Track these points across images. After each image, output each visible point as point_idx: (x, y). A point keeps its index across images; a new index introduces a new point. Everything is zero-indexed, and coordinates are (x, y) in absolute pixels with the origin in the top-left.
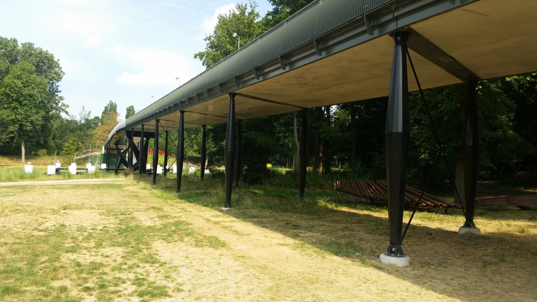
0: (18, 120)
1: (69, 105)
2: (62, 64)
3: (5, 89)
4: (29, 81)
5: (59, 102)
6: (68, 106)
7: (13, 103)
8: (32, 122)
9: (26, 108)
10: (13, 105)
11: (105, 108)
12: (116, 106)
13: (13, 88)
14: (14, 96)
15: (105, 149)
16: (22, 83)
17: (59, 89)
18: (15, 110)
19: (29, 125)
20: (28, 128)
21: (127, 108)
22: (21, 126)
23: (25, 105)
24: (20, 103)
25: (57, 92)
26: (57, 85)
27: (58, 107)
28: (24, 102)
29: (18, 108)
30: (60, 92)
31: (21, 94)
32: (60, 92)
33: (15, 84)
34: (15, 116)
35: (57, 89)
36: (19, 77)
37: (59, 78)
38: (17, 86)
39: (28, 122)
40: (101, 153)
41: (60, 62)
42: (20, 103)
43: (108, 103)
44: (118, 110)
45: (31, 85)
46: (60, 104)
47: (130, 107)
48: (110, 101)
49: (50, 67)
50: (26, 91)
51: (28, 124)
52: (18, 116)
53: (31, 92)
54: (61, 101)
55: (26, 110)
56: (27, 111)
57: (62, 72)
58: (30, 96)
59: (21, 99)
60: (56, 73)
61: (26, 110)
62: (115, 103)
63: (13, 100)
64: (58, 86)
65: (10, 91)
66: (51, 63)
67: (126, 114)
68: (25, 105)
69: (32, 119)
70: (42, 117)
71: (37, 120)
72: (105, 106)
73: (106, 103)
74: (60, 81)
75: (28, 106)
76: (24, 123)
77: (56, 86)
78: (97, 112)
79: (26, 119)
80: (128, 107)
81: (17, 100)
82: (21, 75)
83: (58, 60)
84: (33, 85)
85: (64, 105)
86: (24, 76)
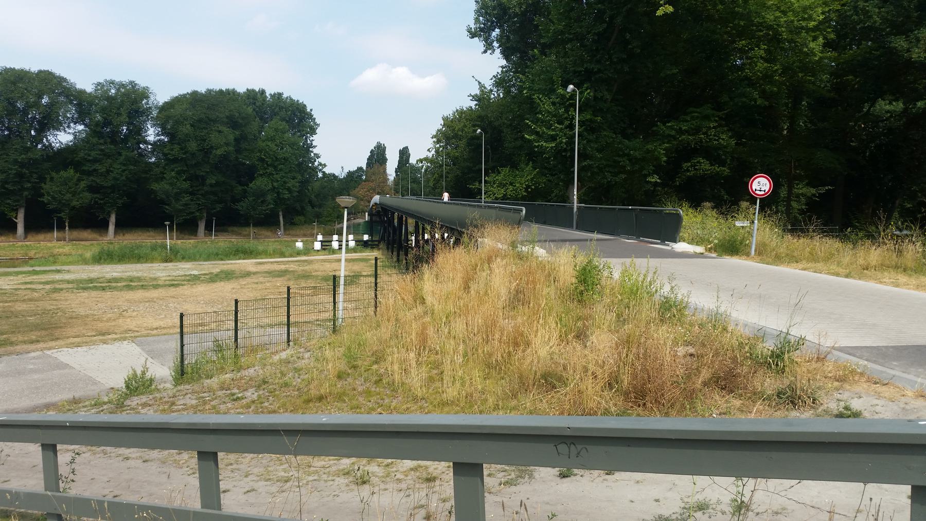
2: (315, 114)
4: (283, 143)
5: (315, 161)
6: (325, 165)
8: (289, 190)
9: (282, 174)
10: (268, 171)
13: (267, 152)
14: (270, 161)
15: (368, 215)
17: (314, 143)
20: (286, 196)
22: (278, 193)
23: (281, 170)
25: (312, 147)
26: (311, 138)
29: (273, 175)
30: (315, 147)
31: (276, 158)
32: (315, 147)
35: (312, 144)
36: (272, 139)
38: (271, 150)
40: (364, 220)
41: (313, 113)
42: (275, 167)
46: (316, 164)
49: (302, 119)
52: (275, 184)
54: (317, 160)
56: (284, 177)
61: (282, 176)
65: (265, 156)
68: (281, 170)
71: (293, 186)
79: (282, 186)
81: (272, 165)
83: (311, 110)
85: (320, 164)
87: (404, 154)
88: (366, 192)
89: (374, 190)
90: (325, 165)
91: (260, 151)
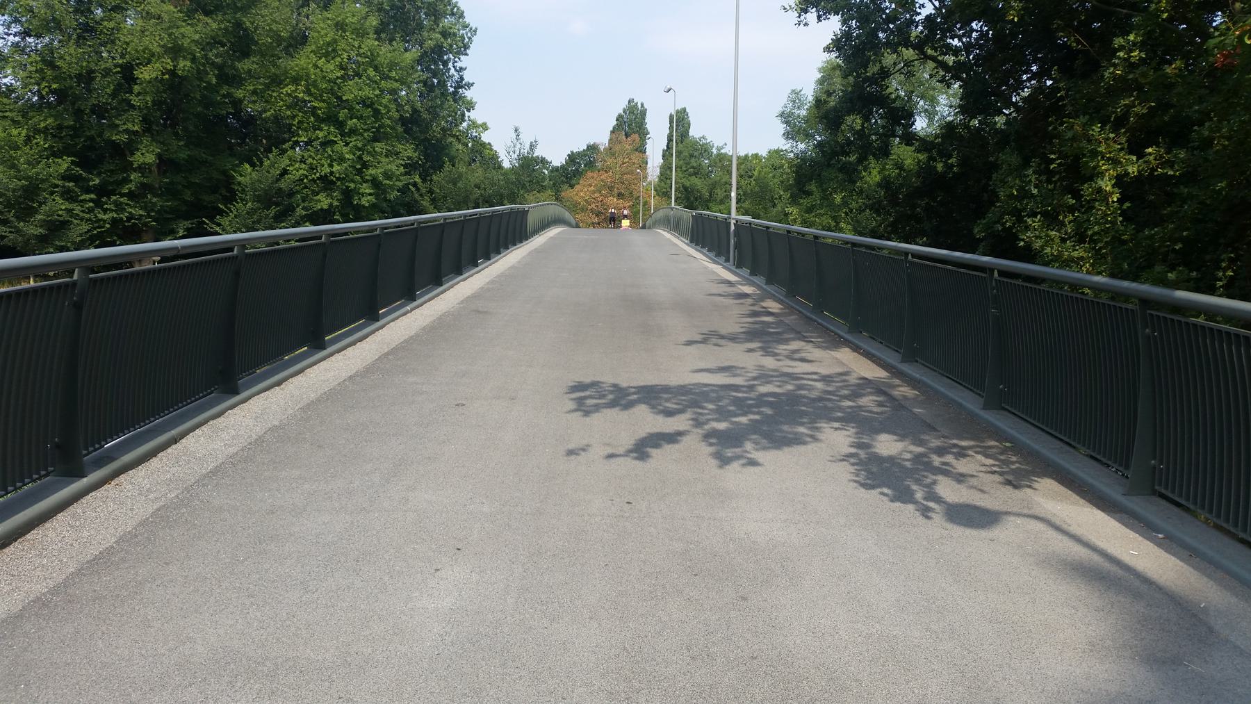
0: (338, 179)
1: (489, 125)
3: (293, 88)
6: (485, 127)
7: (321, 130)
8: (375, 183)
9: (355, 141)
10: (321, 134)
16: (341, 67)
17: (468, 78)
18: (329, 150)
19: (368, 191)
23: (353, 132)
24: (340, 125)
26: (459, 65)
27: (460, 131)
28: (350, 122)
29: (335, 142)
30: (469, 85)
31: (339, 98)
32: (469, 85)
33: (322, 71)
34: (331, 166)
35: (462, 78)
37: (464, 49)
38: (324, 77)
39: (366, 181)
42: (340, 125)
43: (624, 104)
45: (365, 71)
48: (629, 102)
50: (352, 91)
51: (366, 189)
53: (367, 92)
55: (356, 146)
57: (465, 26)
58: (365, 103)
59: (343, 114)
60: (445, 34)
61: (356, 146)
63: (320, 120)
64: (461, 69)
65: (308, 92)
68: (353, 132)
69: (373, 172)
70: (405, 166)
71: (388, 175)
73: (619, 107)
74: (467, 54)
76: (352, 185)
77: (456, 70)
79: (359, 172)
81: (331, 119)
82: (335, 41)
84: (371, 72)
85: (474, 125)
86: (342, 44)
88: (594, 192)
89: (611, 189)
90: (485, 127)
91: (296, 81)
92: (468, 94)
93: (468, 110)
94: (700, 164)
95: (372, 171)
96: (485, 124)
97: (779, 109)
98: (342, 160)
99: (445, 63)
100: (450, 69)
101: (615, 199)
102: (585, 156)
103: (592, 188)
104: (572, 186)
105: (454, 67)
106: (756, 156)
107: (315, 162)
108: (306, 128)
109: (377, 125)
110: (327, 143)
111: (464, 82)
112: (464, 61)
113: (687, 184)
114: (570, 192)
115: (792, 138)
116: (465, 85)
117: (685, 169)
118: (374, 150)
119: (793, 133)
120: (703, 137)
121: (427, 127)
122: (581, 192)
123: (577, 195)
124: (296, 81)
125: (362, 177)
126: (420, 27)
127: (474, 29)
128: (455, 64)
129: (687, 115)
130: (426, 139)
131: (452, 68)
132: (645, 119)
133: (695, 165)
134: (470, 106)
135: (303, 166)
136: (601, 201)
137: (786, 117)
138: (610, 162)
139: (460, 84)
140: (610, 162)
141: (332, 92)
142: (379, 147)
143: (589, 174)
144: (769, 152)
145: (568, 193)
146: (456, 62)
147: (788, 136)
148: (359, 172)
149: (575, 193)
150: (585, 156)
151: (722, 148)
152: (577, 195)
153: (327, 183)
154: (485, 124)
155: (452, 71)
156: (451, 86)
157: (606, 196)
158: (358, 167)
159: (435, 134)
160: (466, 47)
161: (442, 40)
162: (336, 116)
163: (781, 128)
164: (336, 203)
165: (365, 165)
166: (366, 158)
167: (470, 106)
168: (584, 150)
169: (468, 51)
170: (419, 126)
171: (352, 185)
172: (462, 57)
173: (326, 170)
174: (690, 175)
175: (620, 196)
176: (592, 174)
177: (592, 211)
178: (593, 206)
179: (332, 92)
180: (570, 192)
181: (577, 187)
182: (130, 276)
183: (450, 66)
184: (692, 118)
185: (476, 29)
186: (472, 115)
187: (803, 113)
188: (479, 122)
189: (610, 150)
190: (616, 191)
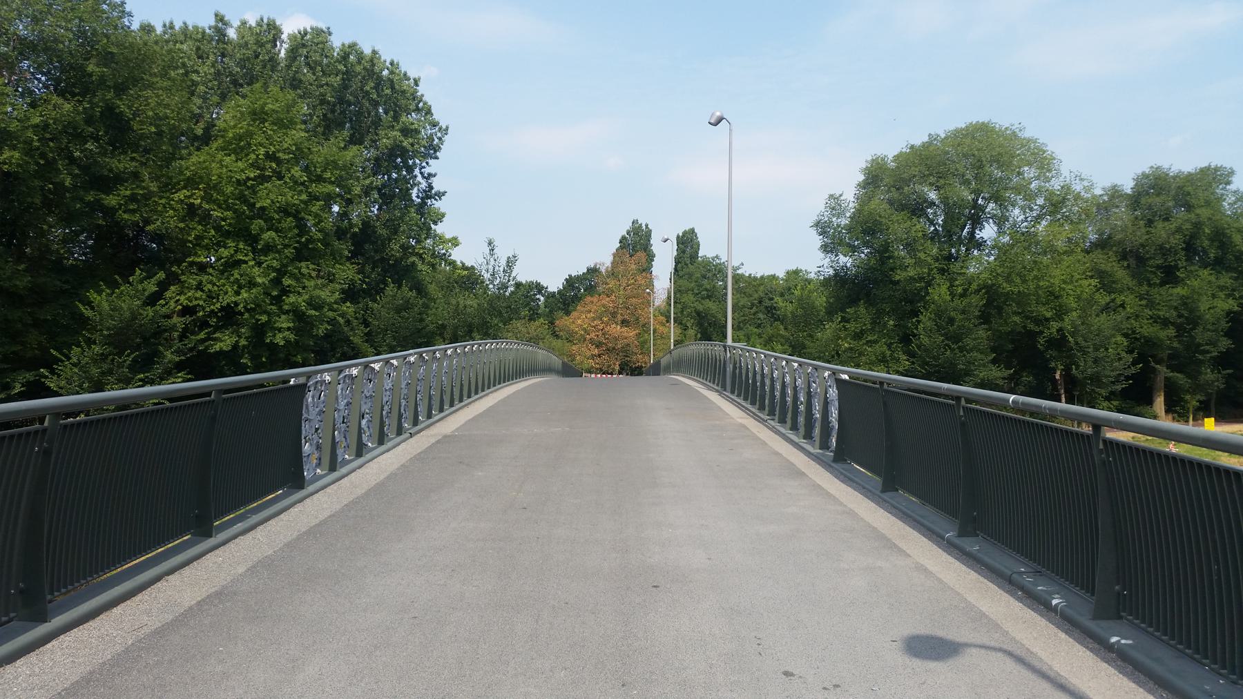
3: (188, 194)
8: (298, 315)
9: (272, 261)
10: (225, 253)
11: (620, 242)
12: (648, 234)
17: (437, 185)
21: (678, 237)
23: (268, 249)
24: (252, 240)
26: (427, 170)
27: (424, 248)
30: (440, 195)
31: (252, 206)
32: (440, 195)
35: (431, 187)
36: (239, 147)
37: (432, 150)
42: (252, 240)
44: (656, 245)
47: (685, 233)
51: (284, 322)
57: (434, 124)
59: (255, 226)
60: (407, 132)
62: (647, 226)
63: (227, 234)
64: (430, 175)
66: (388, 91)
67: (675, 253)
68: (268, 249)
72: (620, 237)
74: (437, 158)
75: (278, 252)
77: (423, 177)
78: (602, 254)
80: (681, 235)
81: (242, 232)
87: (687, 243)
91: (191, 183)
92: (437, 204)
93: (435, 223)
94: (714, 286)
95: (292, 299)
96: (455, 239)
97: (814, 218)
98: (252, 284)
99: (410, 169)
100: (416, 176)
101: (619, 327)
102: (586, 279)
103: (592, 315)
104: (568, 313)
105: (421, 173)
106: (774, 277)
107: (216, 288)
108: (207, 244)
109: (303, 240)
110: (232, 264)
111: (433, 192)
112: (433, 166)
113: (700, 308)
114: (566, 320)
115: (831, 252)
116: (436, 194)
117: (697, 292)
118: (300, 272)
119: (832, 243)
120: (717, 257)
121: (383, 245)
122: (579, 320)
123: (573, 322)
124: (191, 183)
125: (280, 308)
126: (377, 122)
127: (444, 127)
128: (423, 170)
129: (696, 236)
130: (382, 259)
131: (419, 175)
132: (649, 241)
133: (708, 287)
134: (439, 218)
135: (199, 294)
136: (602, 330)
137: (822, 227)
138: (612, 283)
139: (429, 194)
140: (612, 283)
141: (242, 199)
142: (305, 267)
143: (589, 299)
144: (787, 273)
145: (563, 322)
146: (424, 167)
147: (826, 249)
148: (277, 300)
149: (571, 320)
150: (586, 279)
151: (738, 268)
152: (573, 322)
153: (229, 316)
154: (455, 239)
155: (419, 178)
156: (418, 197)
157: (607, 324)
158: (275, 293)
159: (393, 252)
160: (436, 149)
161: (402, 138)
162: (247, 229)
163: (817, 241)
164: (243, 342)
165: (285, 292)
166: (287, 281)
167: (439, 218)
168: (583, 273)
169: (438, 154)
170: (373, 243)
171: (264, 318)
172: (431, 162)
173: (230, 298)
174: (703, 298)
175: (624, 323)
176: (592, 299)
177: (591, 340)
178: (593, 335)
179: (242, 199)
180: (566, 320)
181: (574, 314)
182: (75, 426)
183: (417, 172)
184: (702, 238)
185: (447, 128)
186: (439, 229)
187: (844, 221)
188: (448, 236)
189: (613, 273)
190: (620, 318)
